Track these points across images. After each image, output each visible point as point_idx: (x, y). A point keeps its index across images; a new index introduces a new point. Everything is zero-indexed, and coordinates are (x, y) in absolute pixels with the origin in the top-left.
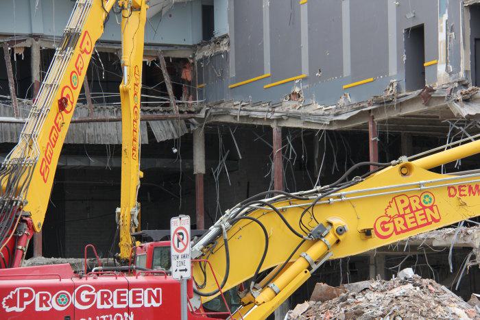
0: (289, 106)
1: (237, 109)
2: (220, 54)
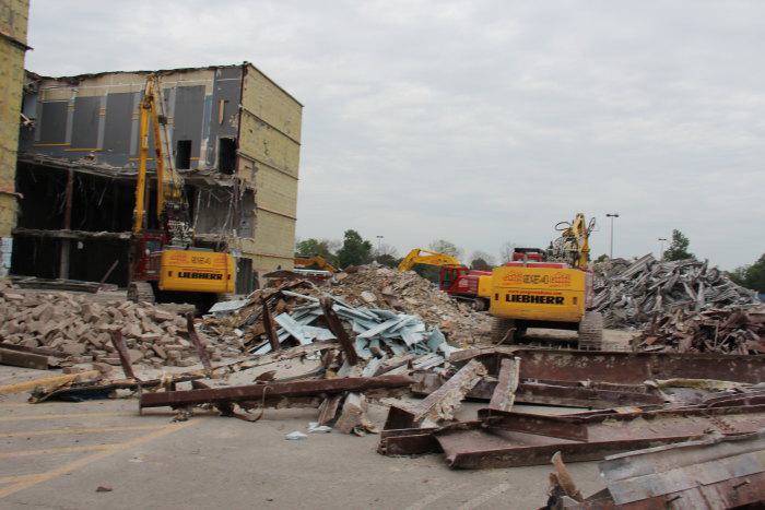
0: (83, 162)
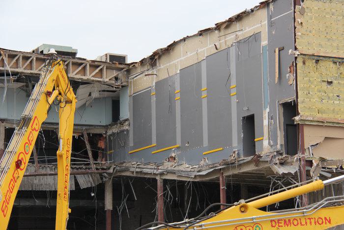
0: (168, 165)
1: (134, 167)
2: (123, 131)
